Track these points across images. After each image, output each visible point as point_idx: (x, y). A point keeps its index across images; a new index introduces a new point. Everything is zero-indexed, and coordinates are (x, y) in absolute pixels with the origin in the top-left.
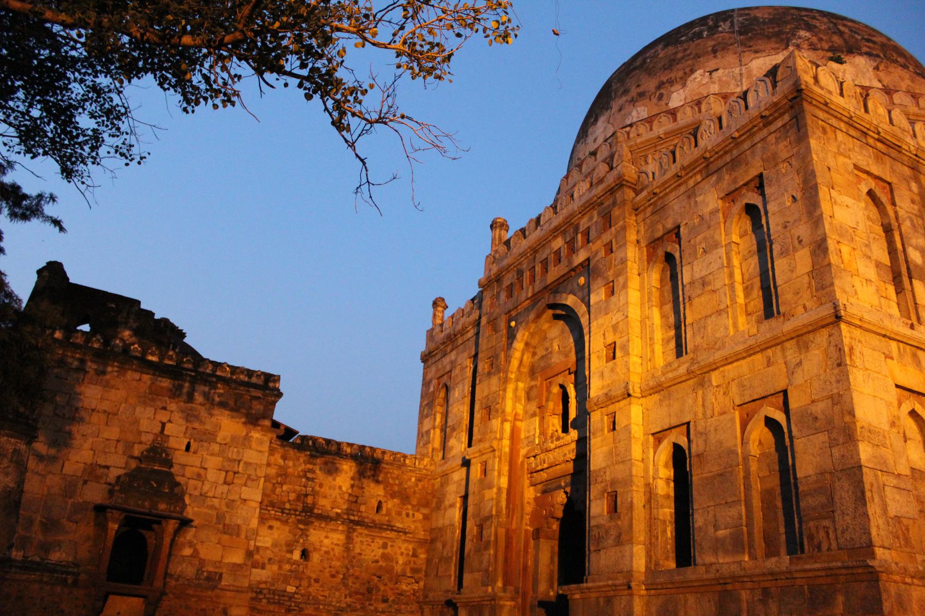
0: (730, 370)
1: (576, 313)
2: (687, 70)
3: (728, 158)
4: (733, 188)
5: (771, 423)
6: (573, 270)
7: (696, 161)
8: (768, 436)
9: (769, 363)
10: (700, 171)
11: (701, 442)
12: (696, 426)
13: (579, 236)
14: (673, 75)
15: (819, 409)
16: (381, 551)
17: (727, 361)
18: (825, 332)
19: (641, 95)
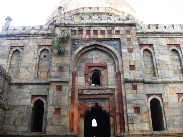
13: (114, 31)
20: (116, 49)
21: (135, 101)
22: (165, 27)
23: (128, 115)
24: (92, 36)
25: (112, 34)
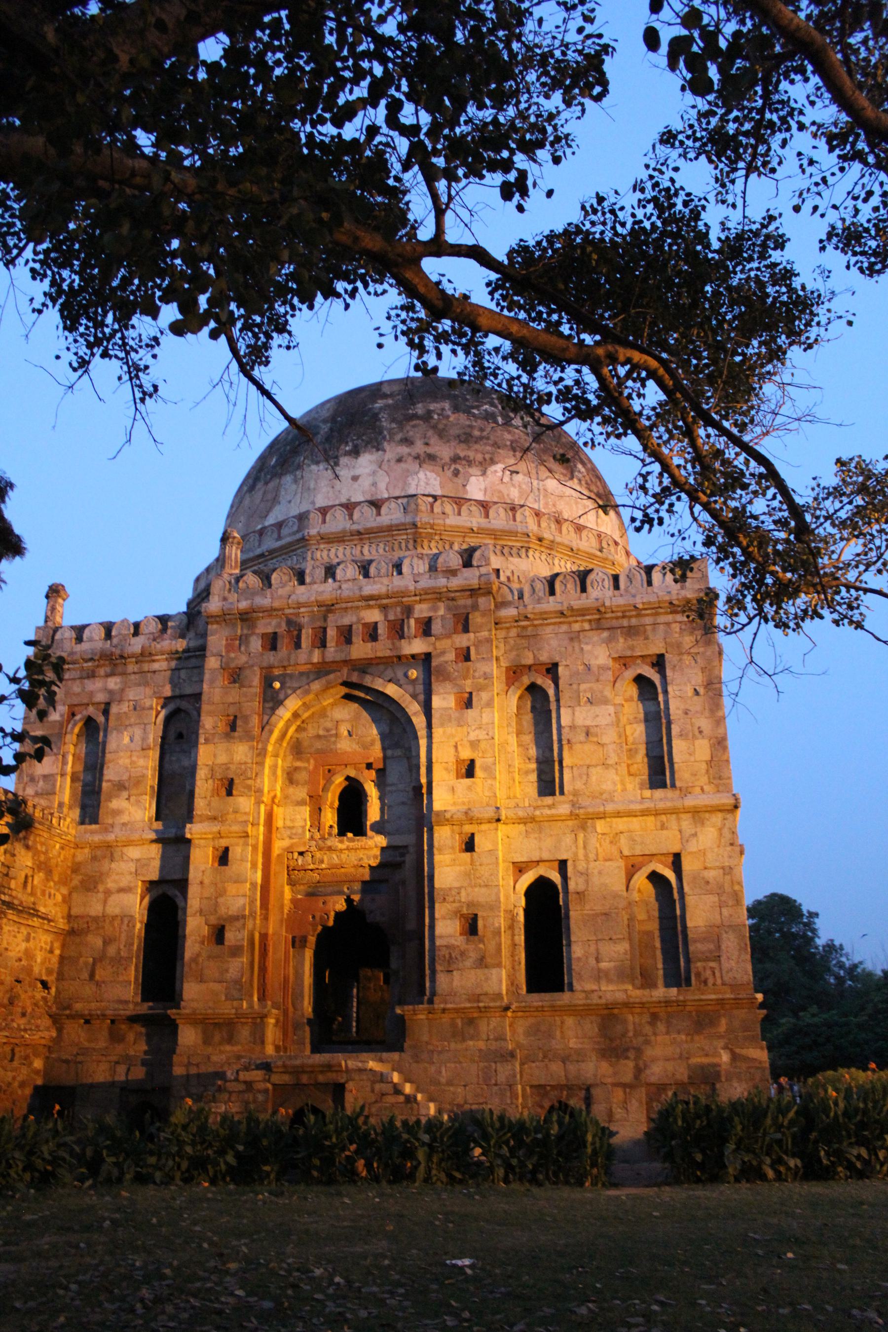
0: (621, 824)
1: (403, 710)
2: (487, 456)
3: (625, 623)
4: (629, 653)
5: (655, 878)
6: (399, 658)
7: (588, 609)
8: (649, 889)
9: (663, 827)
10: (590, 621)
11: (581, 880)
12: (575, 866)
13: (412, 622)
14: (471, 454)
15: (710, 875)
16: (24, 945)
17: (618, 815)
18: (720, 815)
19: (431, 457)
20: (414, 696)
21: (463, 893)
23: (438, 942)
24: (332, 652)
25: (402, 637)
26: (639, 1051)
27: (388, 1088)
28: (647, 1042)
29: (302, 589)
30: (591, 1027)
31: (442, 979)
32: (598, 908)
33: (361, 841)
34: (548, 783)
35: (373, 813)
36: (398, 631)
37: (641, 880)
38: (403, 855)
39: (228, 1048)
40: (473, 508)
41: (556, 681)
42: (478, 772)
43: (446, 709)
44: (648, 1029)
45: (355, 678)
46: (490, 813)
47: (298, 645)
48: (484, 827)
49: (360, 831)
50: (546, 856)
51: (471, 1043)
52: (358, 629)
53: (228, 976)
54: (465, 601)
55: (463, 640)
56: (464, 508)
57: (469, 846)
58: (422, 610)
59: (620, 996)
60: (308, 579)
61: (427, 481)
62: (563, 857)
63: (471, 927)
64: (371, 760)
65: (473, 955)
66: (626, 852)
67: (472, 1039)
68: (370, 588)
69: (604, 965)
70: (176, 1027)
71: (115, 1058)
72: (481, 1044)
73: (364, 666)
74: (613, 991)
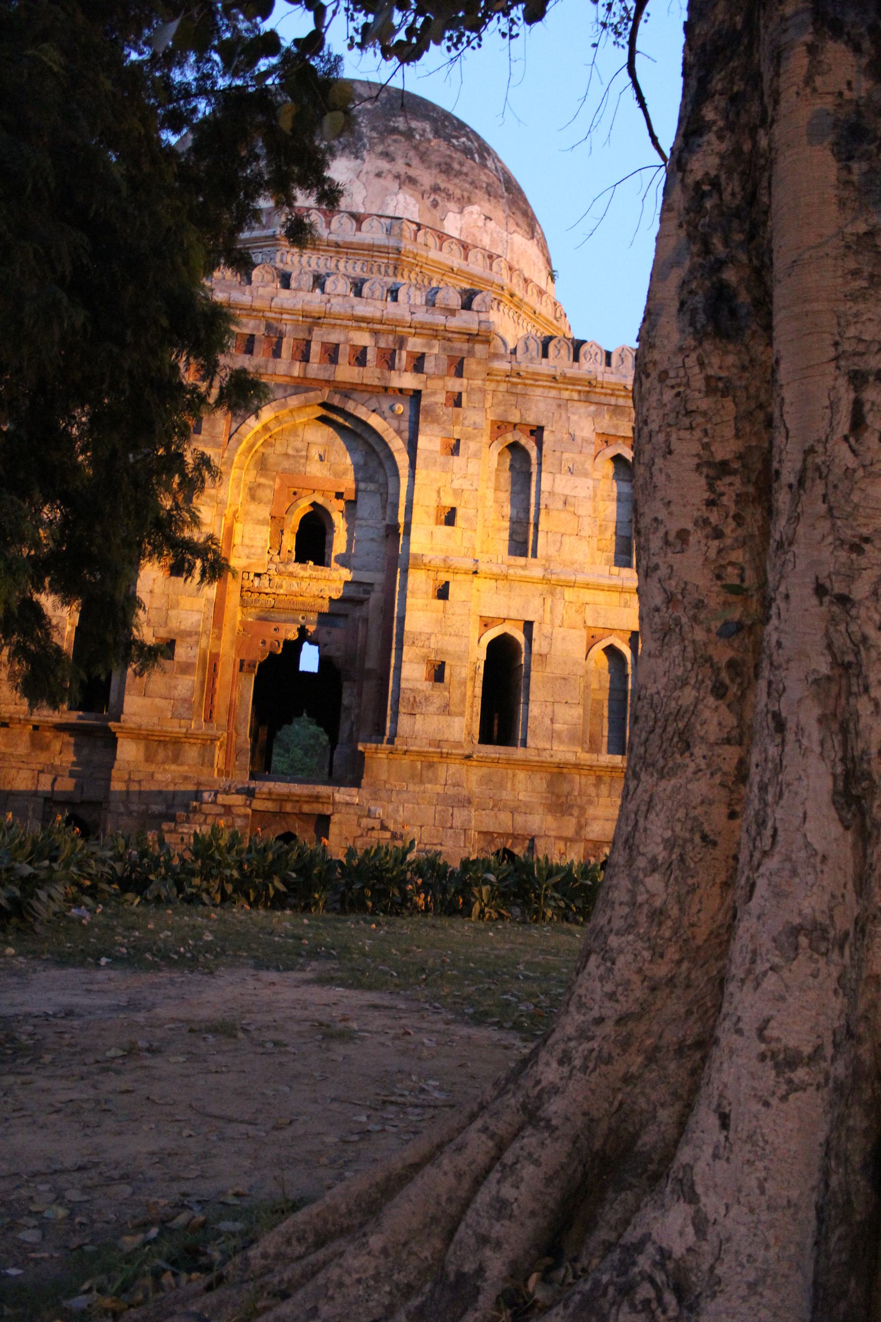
0: (587, 595)
1: (386, 445)
2: (466, 194)
3: (613, 401)
4: (612, 431)
5: (612, 652)
6: (386, 389)
7: (580, 379)
10: (579, 392)
11: (545, 644)
12: (540, 629)
13: (404, 354)
14: (451, 188)
17: (587, 586)
19: (412, 181)
20: (399, 432)
21: (433, 640)
22: (608, 355)
23: (403, 685)
24: (315, 368)
25: (392, 367)
26: (583, 810)
27: (376, 824)
28: (590, 802)
29: (285, 293)
30: (540, 782)
31: (404, 721)
32: (558, 672)
33: (321, 572)
34: (521, 543)
35: (339, 544)
36: (388, 360)
37: (598, 650)
38: (369, 593)
39: (173, 767)
40: (454, 247)
41: (540, 444)
42: (459, 520)
43: (432, 452)
44: (592, 791)
45: (336, 401)
46: (469, 564)
47: (277, 354)
48: (459, 577)
49: (321, 560)
50: (513, 615)
51: (429, 786)
52: (344, 350)
53: (176, 693)
54: (461, 346)
55: (455, 385)
56: (445, 244)
57: (443, 593)
58: (415, 344)
59: (571, 758)
60: (293, 284)
61: (406, 205)
62: (529, 618)
63: (438, 673)
64: (342, 490)
65: (437, 702)
66: (590, 623)
67: (430, 782)
68: (362, 309)
69: (557, 726)
70: (115, 740)
71: (39, 767)
72: (439, 789)
73: (348, 390)
74: (563, 752)
